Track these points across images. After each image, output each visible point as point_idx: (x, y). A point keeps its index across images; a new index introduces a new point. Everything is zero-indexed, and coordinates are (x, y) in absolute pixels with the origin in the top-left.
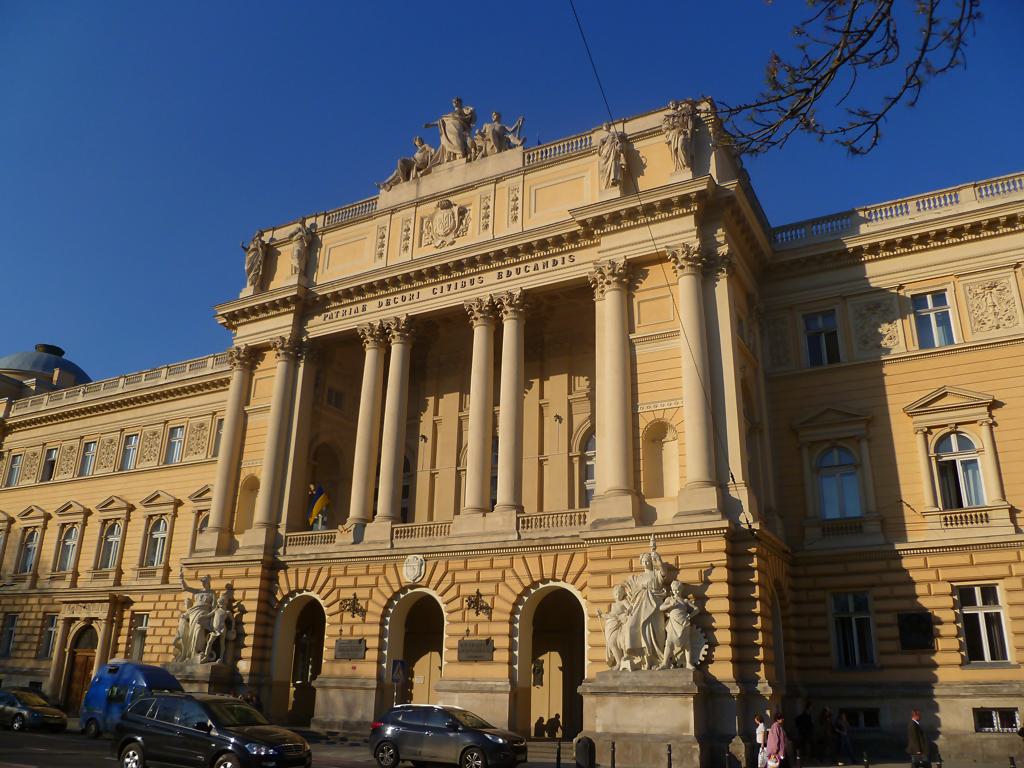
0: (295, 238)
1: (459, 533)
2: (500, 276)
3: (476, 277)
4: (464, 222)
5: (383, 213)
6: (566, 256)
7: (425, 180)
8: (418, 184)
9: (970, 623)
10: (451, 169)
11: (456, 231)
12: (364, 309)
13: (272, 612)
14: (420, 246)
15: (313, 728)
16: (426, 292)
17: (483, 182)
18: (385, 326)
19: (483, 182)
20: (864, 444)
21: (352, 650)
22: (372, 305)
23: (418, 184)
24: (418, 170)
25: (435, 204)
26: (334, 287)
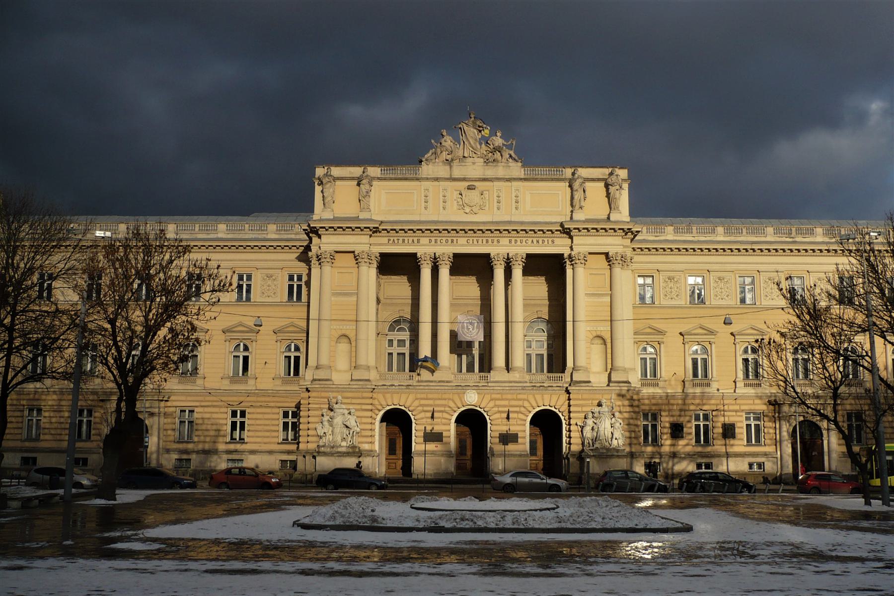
0: (364, 182)
1: (496, 379)
2: (510, 241)
3: (496, 239)
5: (427, 179)
6: (550, 240)
7: (455, 163)
8: (451, 167)
9: (697, 427)
10: (474, 163)
12: (418, 241)
13: (374, 416)
15: (414, 476)
16: (462, 241)
17: (498, 179)
18: (437, 256)
19: (498, 179)
20: (662, 345)
21: (433, 437)
22: (424, 241)
23: (451, 167)
25: (467, 184)
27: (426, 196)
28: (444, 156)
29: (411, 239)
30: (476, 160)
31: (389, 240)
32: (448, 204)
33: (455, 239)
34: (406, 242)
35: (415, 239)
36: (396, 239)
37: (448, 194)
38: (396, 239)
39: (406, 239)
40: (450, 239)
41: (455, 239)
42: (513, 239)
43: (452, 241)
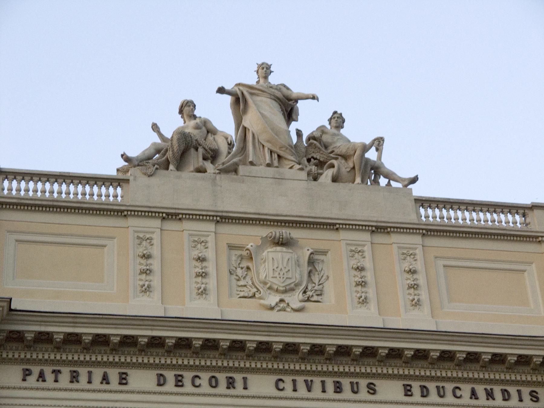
2: (408, 391)
3: (363, 383)
4: (316, 279)
7: (225, 180)
11: (305, 292)
12: (123, 380)
14: (231, 296)
24: (205, 159)
26: (75, 324)
27: (147, 257)
28: (196, 159)
29: (98, 373)
30: (285, 171)
31: (27, 373)
32: (211, 283)
33: (238, 377)
34: (83, 378)
35: (114, 374)
36: (48, 370)
37: (210, 254)
38: (48, 370)
39: (83, 372)
40: (222, 377)
41: (238, 377)
42: (416, 386)
43: (231, 383)
